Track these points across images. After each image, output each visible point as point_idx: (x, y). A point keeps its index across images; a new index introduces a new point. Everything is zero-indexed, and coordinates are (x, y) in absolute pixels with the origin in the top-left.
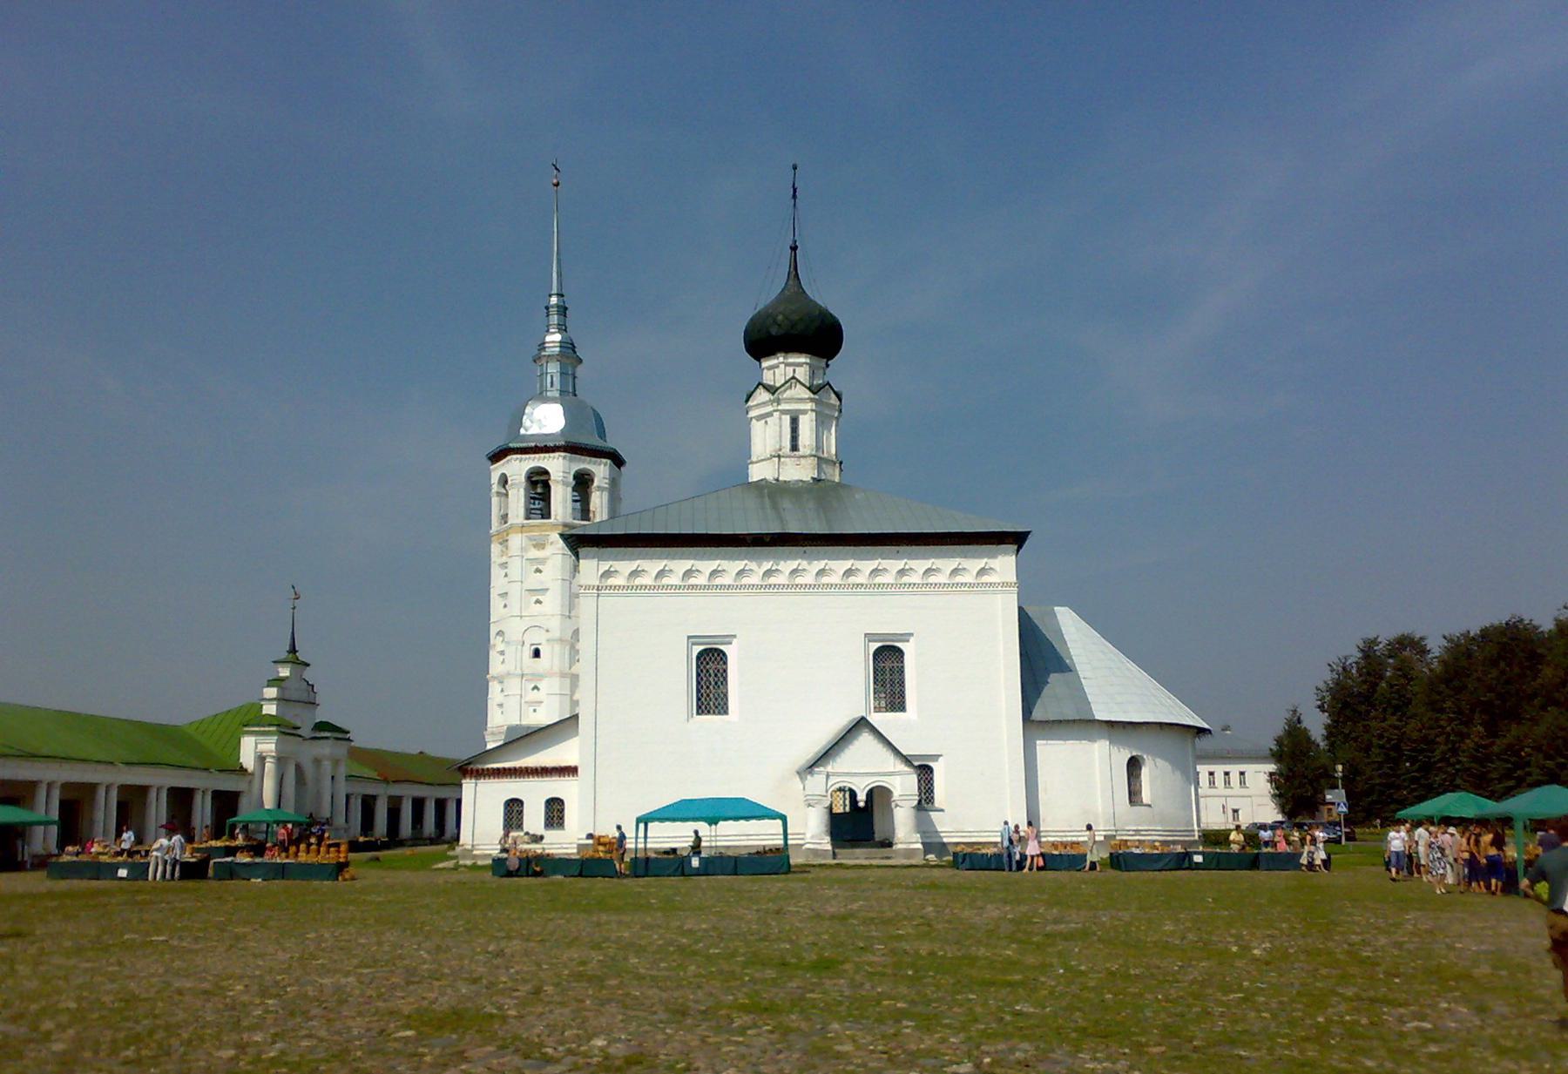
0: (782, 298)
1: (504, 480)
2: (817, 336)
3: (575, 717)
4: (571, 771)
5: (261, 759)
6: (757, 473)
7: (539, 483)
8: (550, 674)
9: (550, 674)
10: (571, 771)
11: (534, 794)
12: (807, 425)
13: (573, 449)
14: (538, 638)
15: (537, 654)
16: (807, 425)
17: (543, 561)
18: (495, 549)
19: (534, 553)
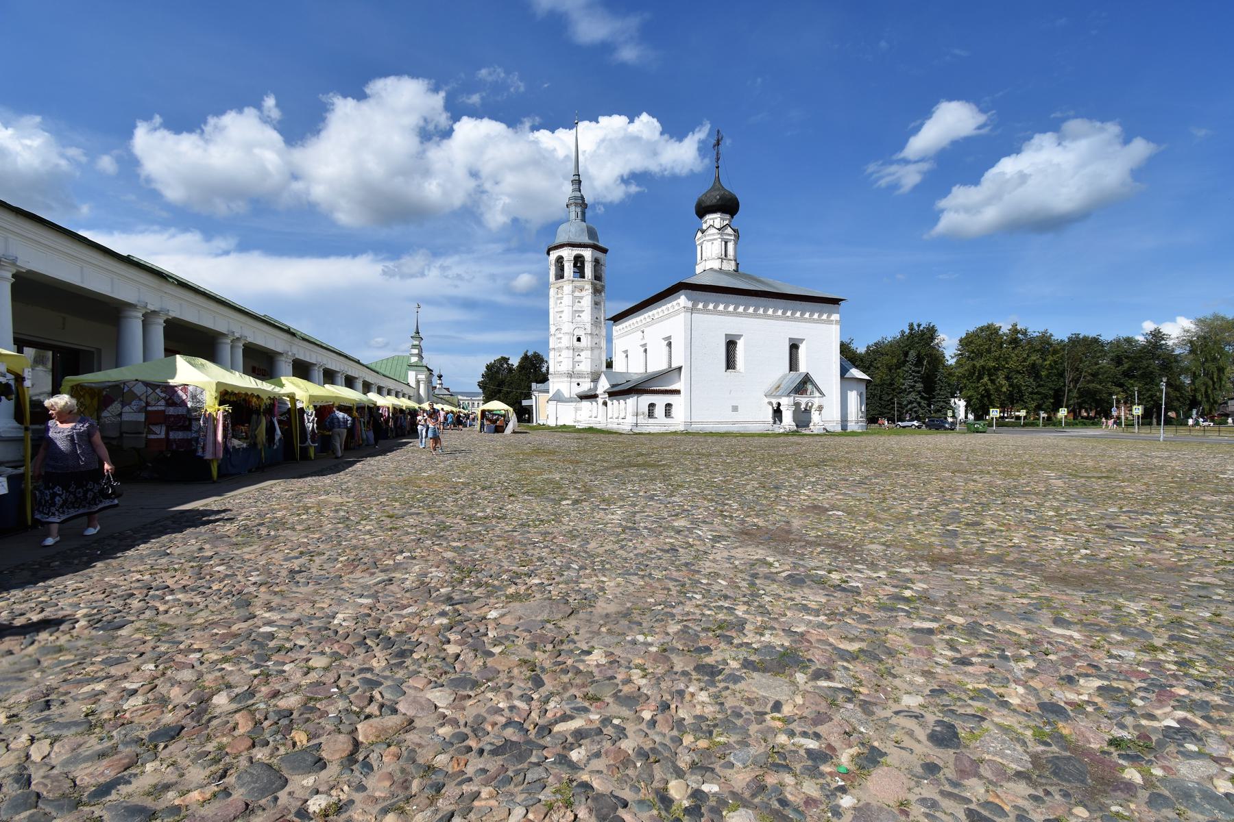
0: (713, 189)
1: (560, 260)
2: (729, 206)
3: (680, 368)
4: (677, 392)
5: (418, 382)
6: (709, 265)
7: (579, 260)
8: (586, 349)
9: (586, 349)
10: (677, 392)
11: (660, 401)
12: (731, 246)
13: (595, 247)
14: (578, 332)
15: (579, 340)
16: (731, 246)
17: (581, 298)
18: (552, 292)
19: (577, 294)
